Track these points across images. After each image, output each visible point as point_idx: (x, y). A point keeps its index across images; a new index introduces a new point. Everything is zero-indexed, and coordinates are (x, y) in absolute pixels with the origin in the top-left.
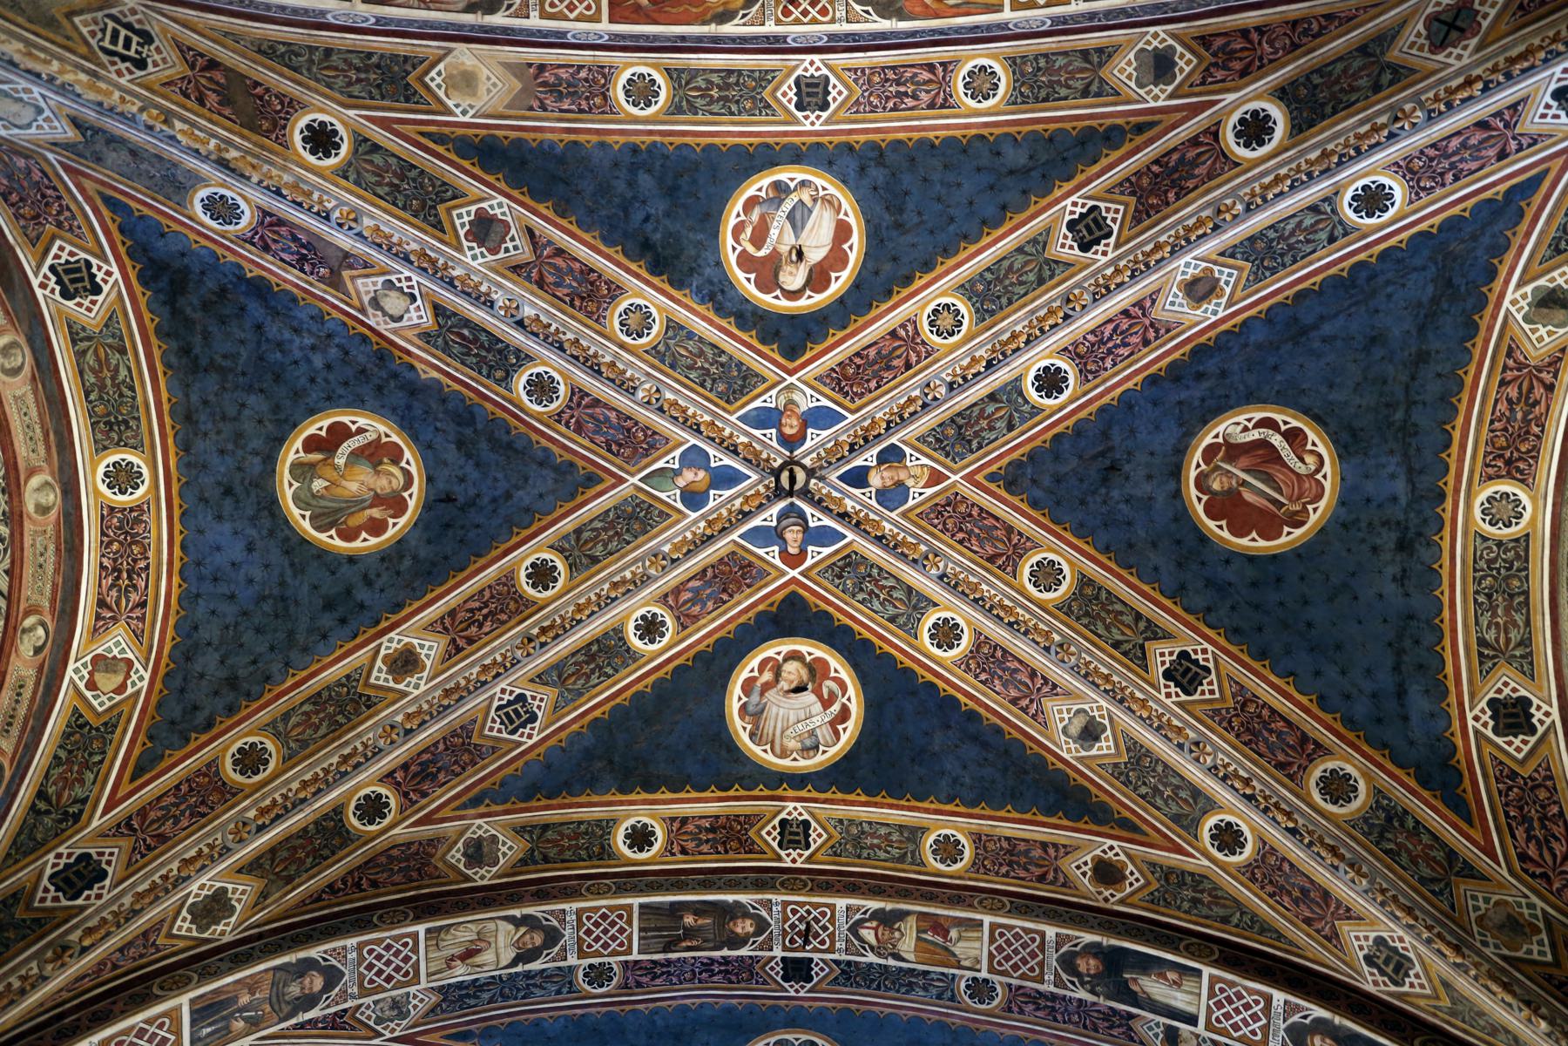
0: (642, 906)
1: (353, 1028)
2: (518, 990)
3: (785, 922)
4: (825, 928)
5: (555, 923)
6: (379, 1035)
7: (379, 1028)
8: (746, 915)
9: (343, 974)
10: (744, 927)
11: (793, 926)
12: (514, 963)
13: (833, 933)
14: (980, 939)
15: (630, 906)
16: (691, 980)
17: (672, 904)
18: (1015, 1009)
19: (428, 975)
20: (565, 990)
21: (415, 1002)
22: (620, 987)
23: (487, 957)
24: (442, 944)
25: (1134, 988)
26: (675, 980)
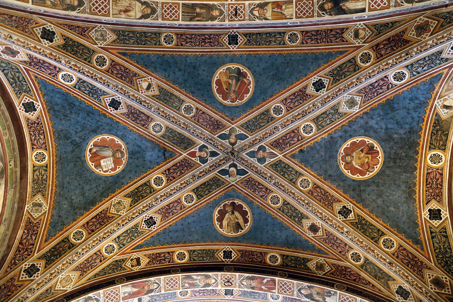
0: (183, 4)
1: (88, 38)
2: (142, 41)
3: (229, 11)
4: (242, 12)
5: (155, 6)
6: (97, 45)
7: (96, 42)
8: (216, 9)
9: (84, 4)
10: (216, 13)
11: (232, 12)
12: (141, 18)
13: (245, 14)
14: (292, 7)
15: (179, 3)
16: (198, 45)
17: (193, 4)
18: (305, 42)
19: (113, 14)
20: (158, 44)
21: (108, 36)
22: (175, 45)
23: (132, 13)
24: (118, 5)
25: (344, 8)
26: (193, 45)
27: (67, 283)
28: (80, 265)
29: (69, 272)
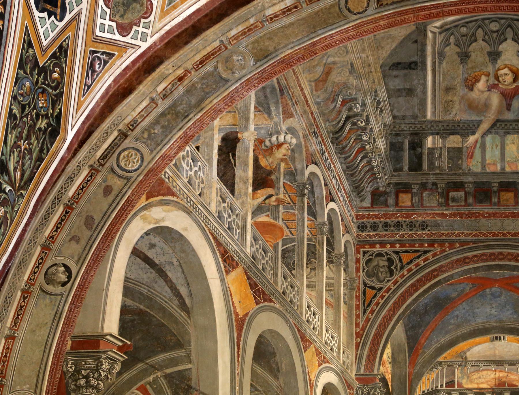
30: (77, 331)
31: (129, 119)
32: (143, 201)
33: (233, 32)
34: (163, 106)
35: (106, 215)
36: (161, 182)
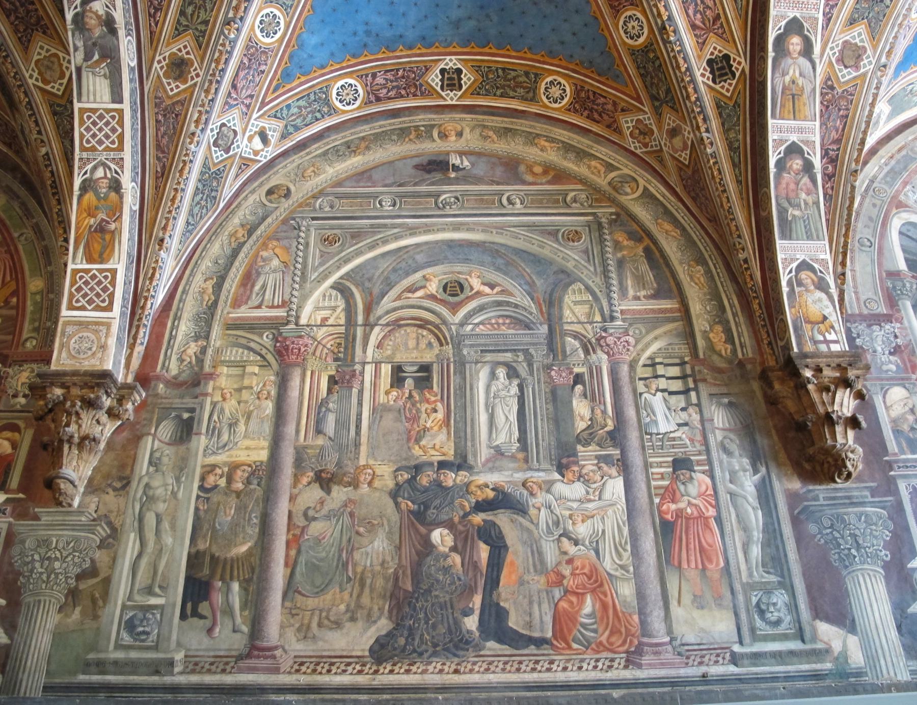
27: (56, 66)
28: (16, 31)
29: (27, 60)
30: (885, 268)
31: (872, 175)
32: (894, 211)
33: (910, 138)
34: (886, 169)
35: (878, 216)
36: (900, 202)
